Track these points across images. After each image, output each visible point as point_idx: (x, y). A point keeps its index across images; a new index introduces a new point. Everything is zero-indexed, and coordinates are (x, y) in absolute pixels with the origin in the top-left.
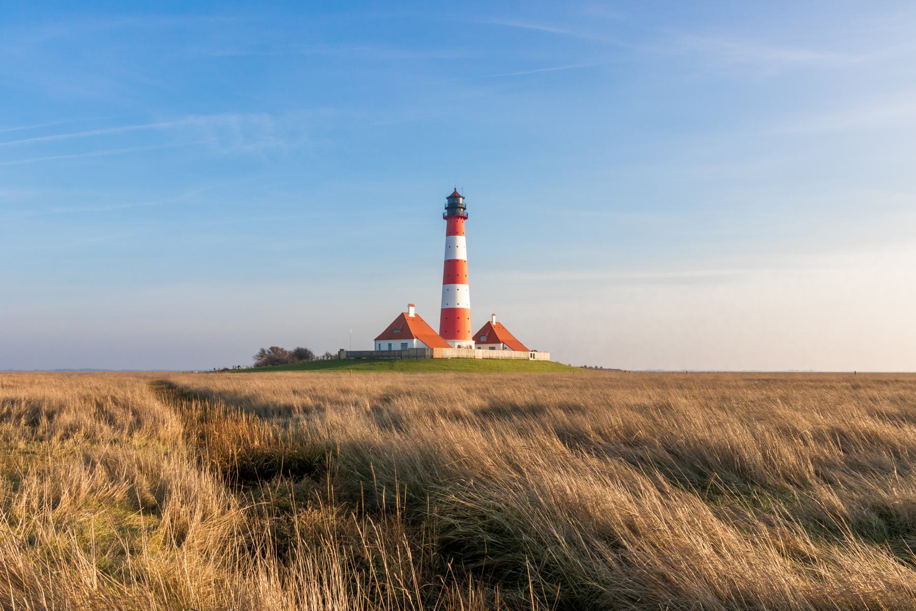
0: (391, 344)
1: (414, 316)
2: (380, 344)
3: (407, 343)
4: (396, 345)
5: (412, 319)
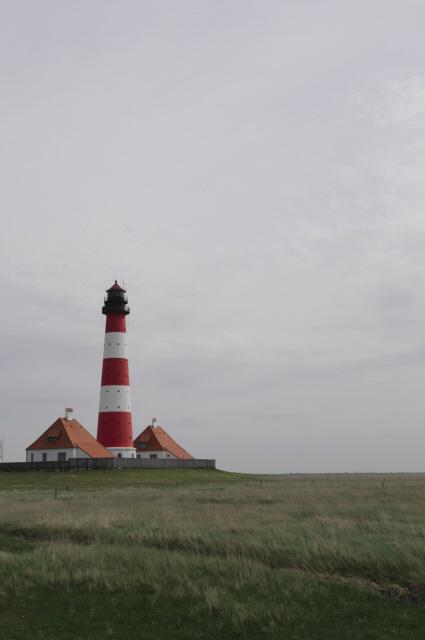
2: (32, 455)
4: (53, 456)
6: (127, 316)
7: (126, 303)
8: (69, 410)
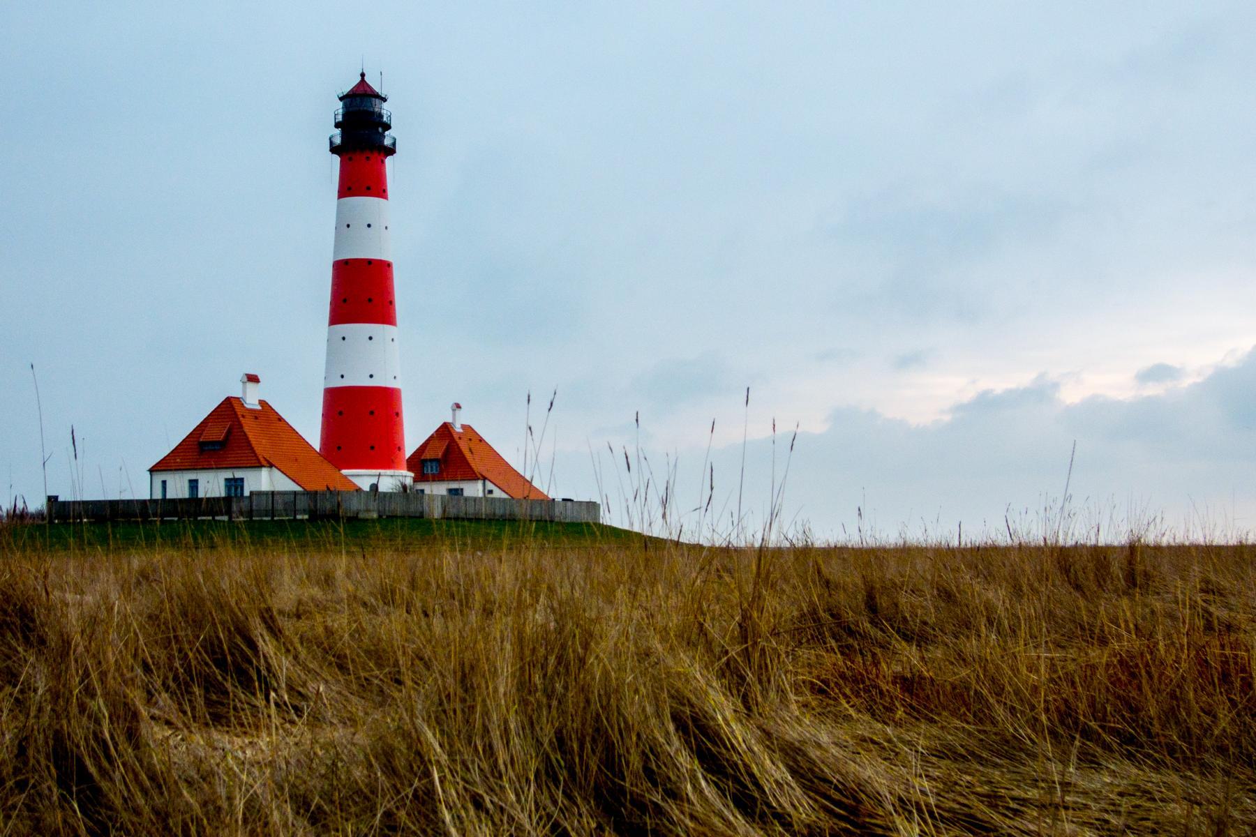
0: (196, 481)
1: (259, 408)
2: (164, 483)
3: (242, 480)
4: (212, 484)
5: (255, 414)
6: (389, 161)
7: (388, 127)
8: (253, 379)
